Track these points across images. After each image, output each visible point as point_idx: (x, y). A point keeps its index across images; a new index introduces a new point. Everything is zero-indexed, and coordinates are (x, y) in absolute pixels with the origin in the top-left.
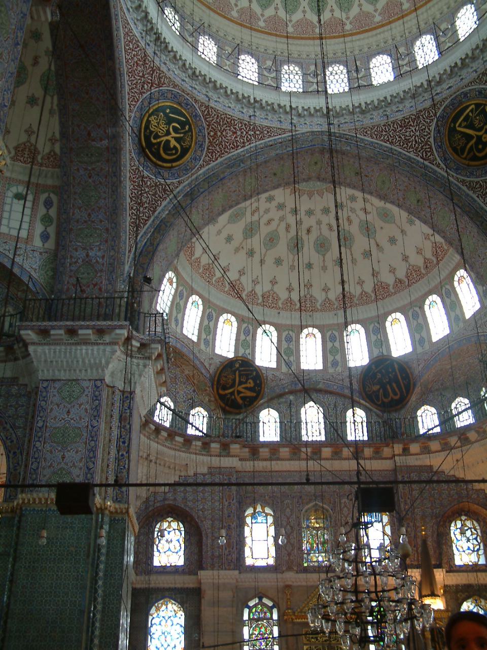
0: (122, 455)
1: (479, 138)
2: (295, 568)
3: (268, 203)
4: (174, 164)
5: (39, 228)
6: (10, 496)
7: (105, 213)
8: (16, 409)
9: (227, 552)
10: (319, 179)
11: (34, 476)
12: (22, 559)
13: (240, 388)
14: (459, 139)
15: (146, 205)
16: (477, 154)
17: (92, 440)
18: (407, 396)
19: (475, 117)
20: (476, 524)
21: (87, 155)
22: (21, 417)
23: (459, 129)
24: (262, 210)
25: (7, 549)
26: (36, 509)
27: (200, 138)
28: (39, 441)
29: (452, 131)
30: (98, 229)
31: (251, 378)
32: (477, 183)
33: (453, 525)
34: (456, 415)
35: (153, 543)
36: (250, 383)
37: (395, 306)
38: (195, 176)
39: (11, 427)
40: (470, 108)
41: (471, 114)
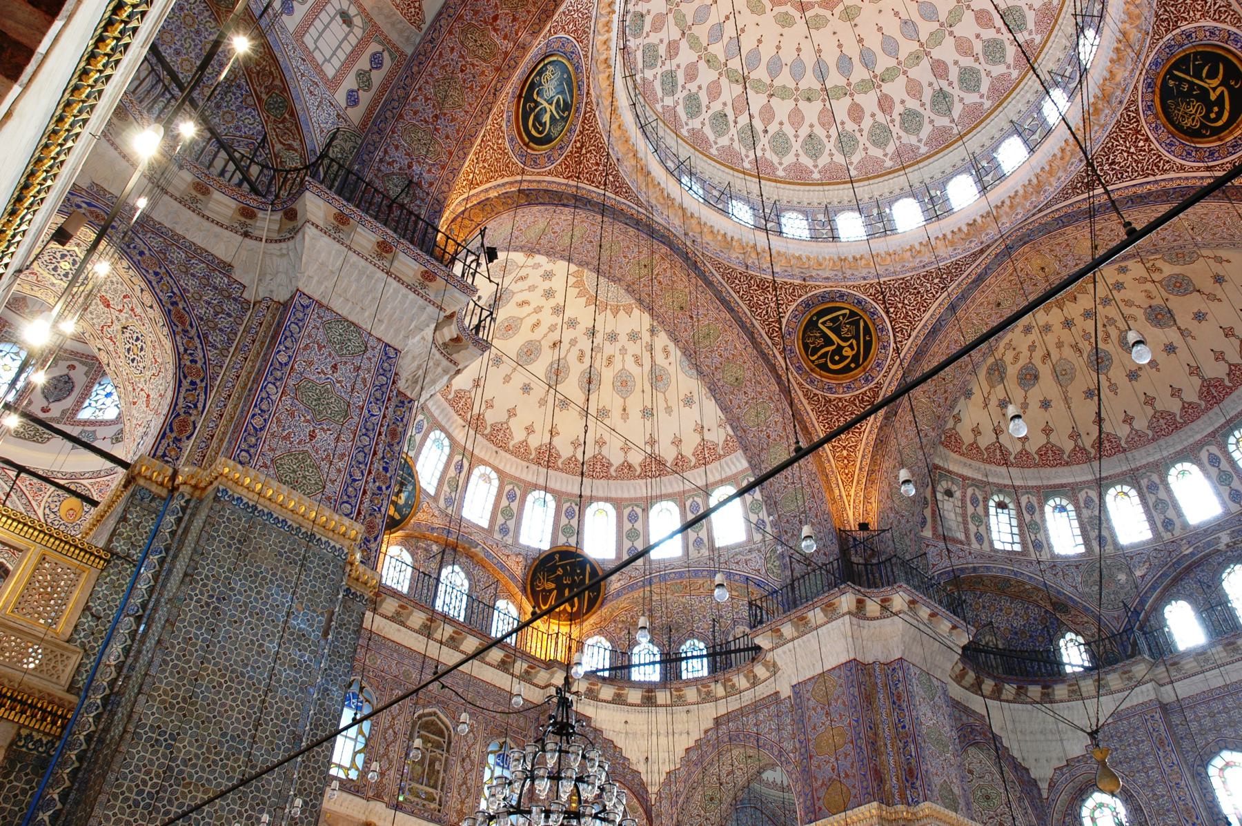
0: (380, 488)
1: (840, 348)
2: (386, 799)
3: (547, 282)
4: (531, 144)
5: (350, 82)
6: (164, 455)
7: (458, 131)
8: (217, 314)
10: (630, 289)
11: (253, 440)
12: (197, 582)
14: (816, 337)
15: (486, 165)
16: (830, 365)
17: (365, 435)
18: (586, 613)
19: (846, 324)
21: (476, 41)
22: (221, 330)
23: (820, 325)
24: (528, 282)
25: (132, 552)
26: (245, 500)
27: (565, 139)
28: (274, 384)
29: (811, 325)
30: (439, 144)
32: (816, 395)
34: (635, 666)
38: (473, 192)
39: (199, 337)
40: (843, 312)
41: (841, 318)
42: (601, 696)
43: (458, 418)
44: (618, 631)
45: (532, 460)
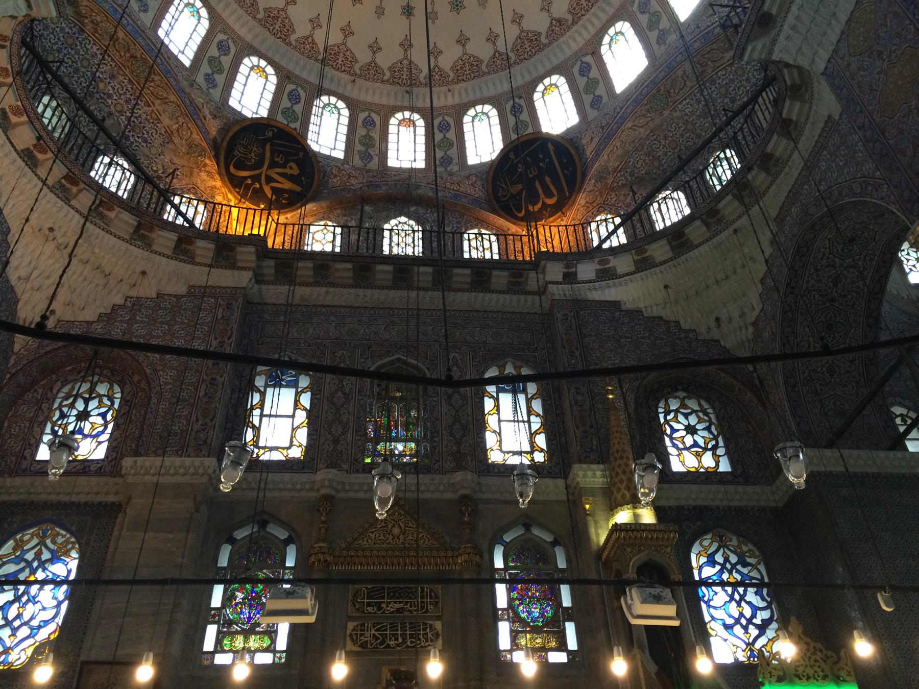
9: (197, 427)
13: (273, 173)
18: (570, 196)
20: (706, 405)
31: (296, 162)
33: (662, 404)
35: (48, 418)
36: (291, 168)
37: (549, 66)
42: (620, 271)
43: (343, 75)
44: (622, 198)
45: (452, 81)
